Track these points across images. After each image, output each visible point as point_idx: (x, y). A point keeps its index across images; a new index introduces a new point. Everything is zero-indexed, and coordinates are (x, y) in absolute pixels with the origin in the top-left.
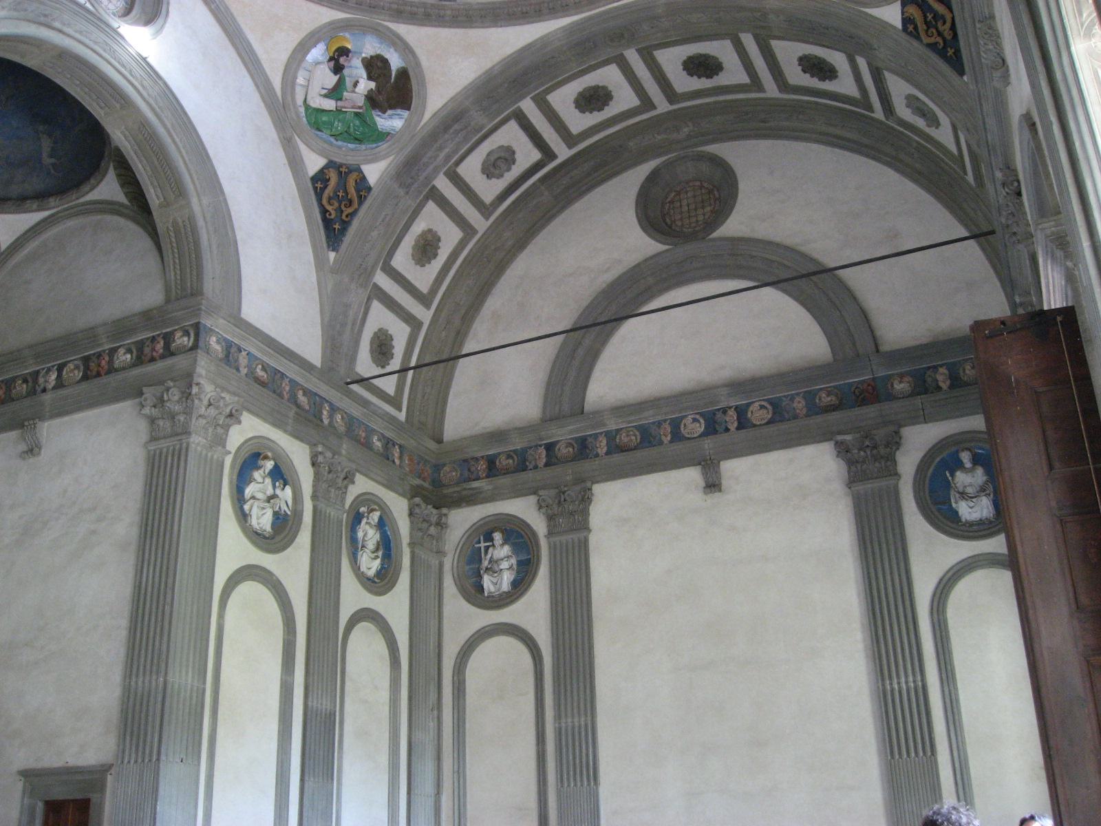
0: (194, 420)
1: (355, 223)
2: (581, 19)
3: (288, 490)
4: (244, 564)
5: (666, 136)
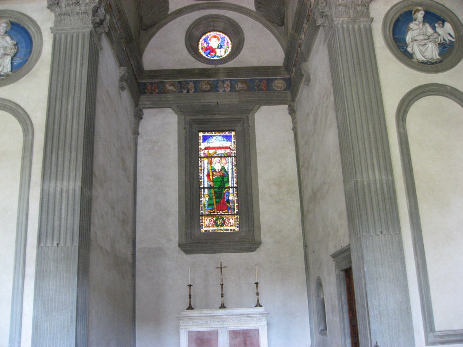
0: (334, 11)
3: (448, 25)
4: (415, 86)
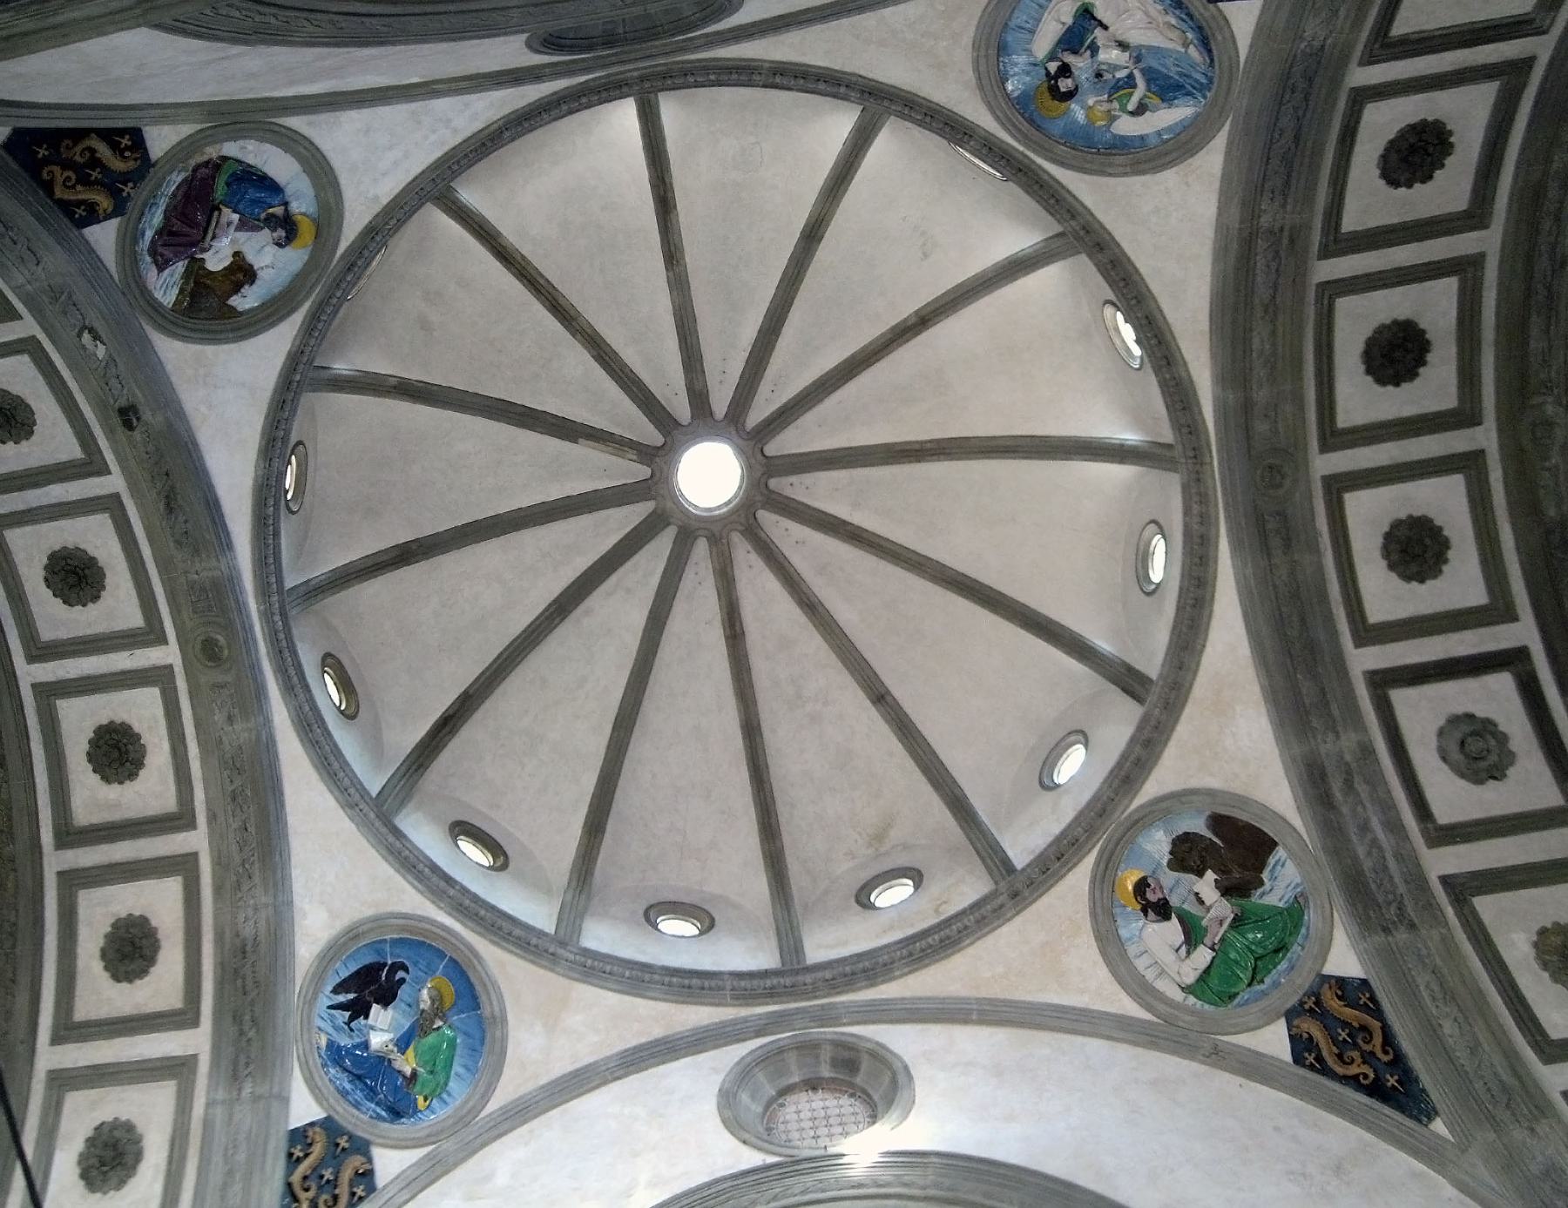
1: (1406, 1046)
2: (1226, 522)
5: (1556, 448)
